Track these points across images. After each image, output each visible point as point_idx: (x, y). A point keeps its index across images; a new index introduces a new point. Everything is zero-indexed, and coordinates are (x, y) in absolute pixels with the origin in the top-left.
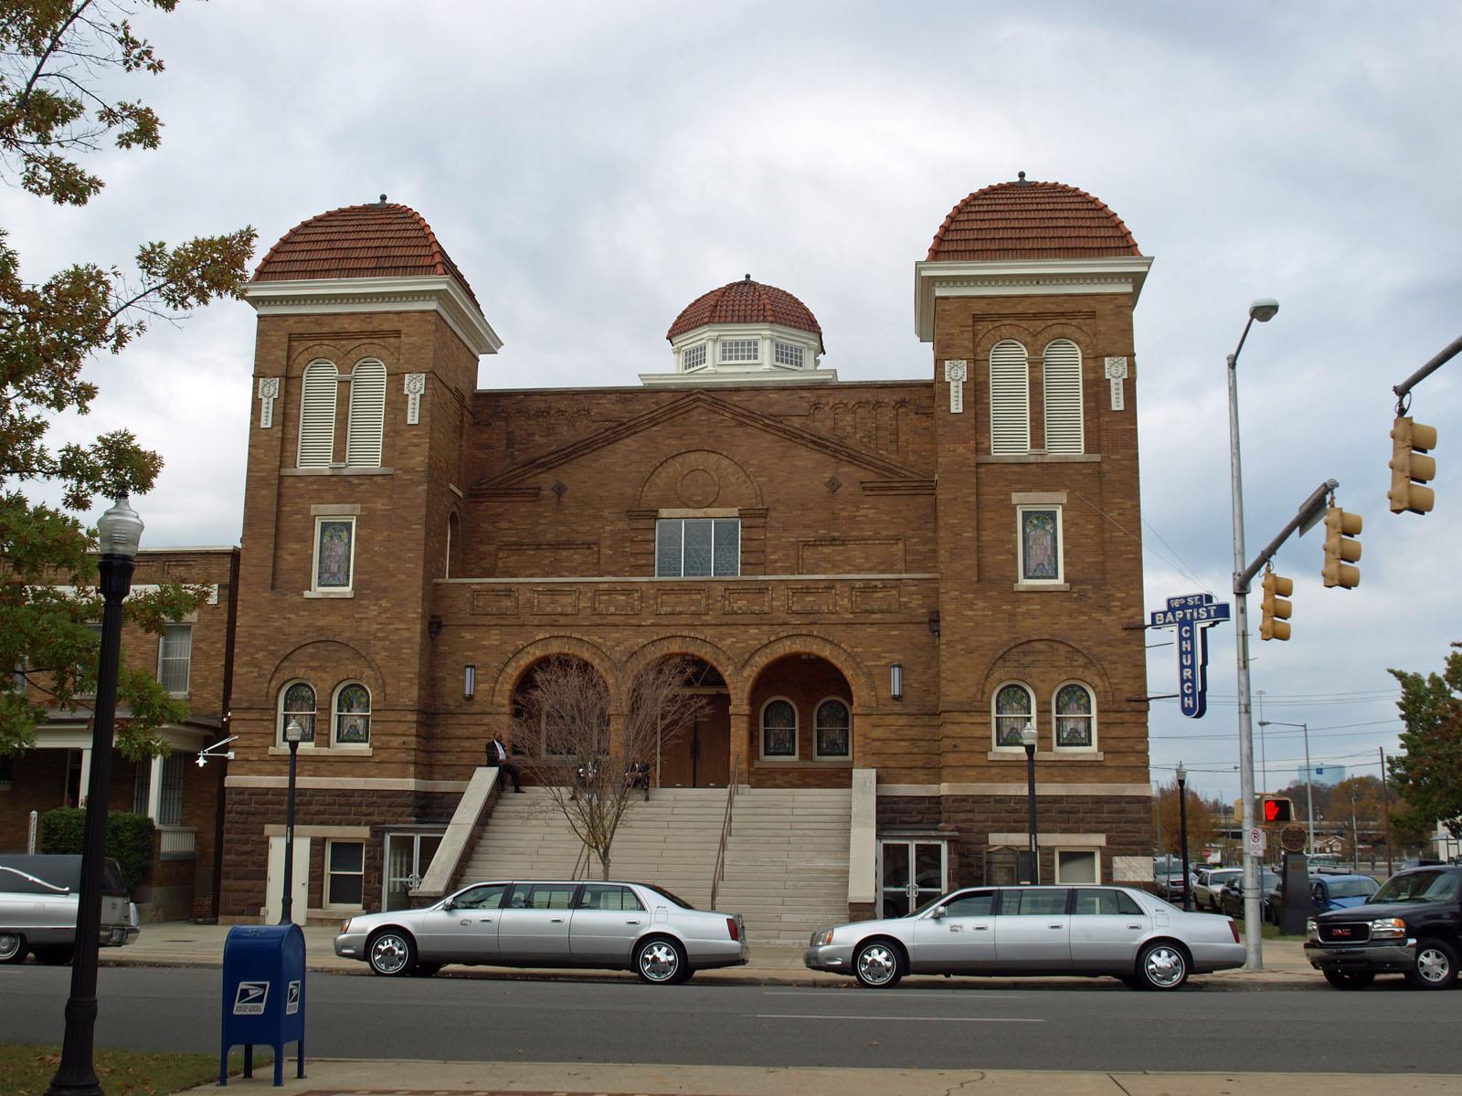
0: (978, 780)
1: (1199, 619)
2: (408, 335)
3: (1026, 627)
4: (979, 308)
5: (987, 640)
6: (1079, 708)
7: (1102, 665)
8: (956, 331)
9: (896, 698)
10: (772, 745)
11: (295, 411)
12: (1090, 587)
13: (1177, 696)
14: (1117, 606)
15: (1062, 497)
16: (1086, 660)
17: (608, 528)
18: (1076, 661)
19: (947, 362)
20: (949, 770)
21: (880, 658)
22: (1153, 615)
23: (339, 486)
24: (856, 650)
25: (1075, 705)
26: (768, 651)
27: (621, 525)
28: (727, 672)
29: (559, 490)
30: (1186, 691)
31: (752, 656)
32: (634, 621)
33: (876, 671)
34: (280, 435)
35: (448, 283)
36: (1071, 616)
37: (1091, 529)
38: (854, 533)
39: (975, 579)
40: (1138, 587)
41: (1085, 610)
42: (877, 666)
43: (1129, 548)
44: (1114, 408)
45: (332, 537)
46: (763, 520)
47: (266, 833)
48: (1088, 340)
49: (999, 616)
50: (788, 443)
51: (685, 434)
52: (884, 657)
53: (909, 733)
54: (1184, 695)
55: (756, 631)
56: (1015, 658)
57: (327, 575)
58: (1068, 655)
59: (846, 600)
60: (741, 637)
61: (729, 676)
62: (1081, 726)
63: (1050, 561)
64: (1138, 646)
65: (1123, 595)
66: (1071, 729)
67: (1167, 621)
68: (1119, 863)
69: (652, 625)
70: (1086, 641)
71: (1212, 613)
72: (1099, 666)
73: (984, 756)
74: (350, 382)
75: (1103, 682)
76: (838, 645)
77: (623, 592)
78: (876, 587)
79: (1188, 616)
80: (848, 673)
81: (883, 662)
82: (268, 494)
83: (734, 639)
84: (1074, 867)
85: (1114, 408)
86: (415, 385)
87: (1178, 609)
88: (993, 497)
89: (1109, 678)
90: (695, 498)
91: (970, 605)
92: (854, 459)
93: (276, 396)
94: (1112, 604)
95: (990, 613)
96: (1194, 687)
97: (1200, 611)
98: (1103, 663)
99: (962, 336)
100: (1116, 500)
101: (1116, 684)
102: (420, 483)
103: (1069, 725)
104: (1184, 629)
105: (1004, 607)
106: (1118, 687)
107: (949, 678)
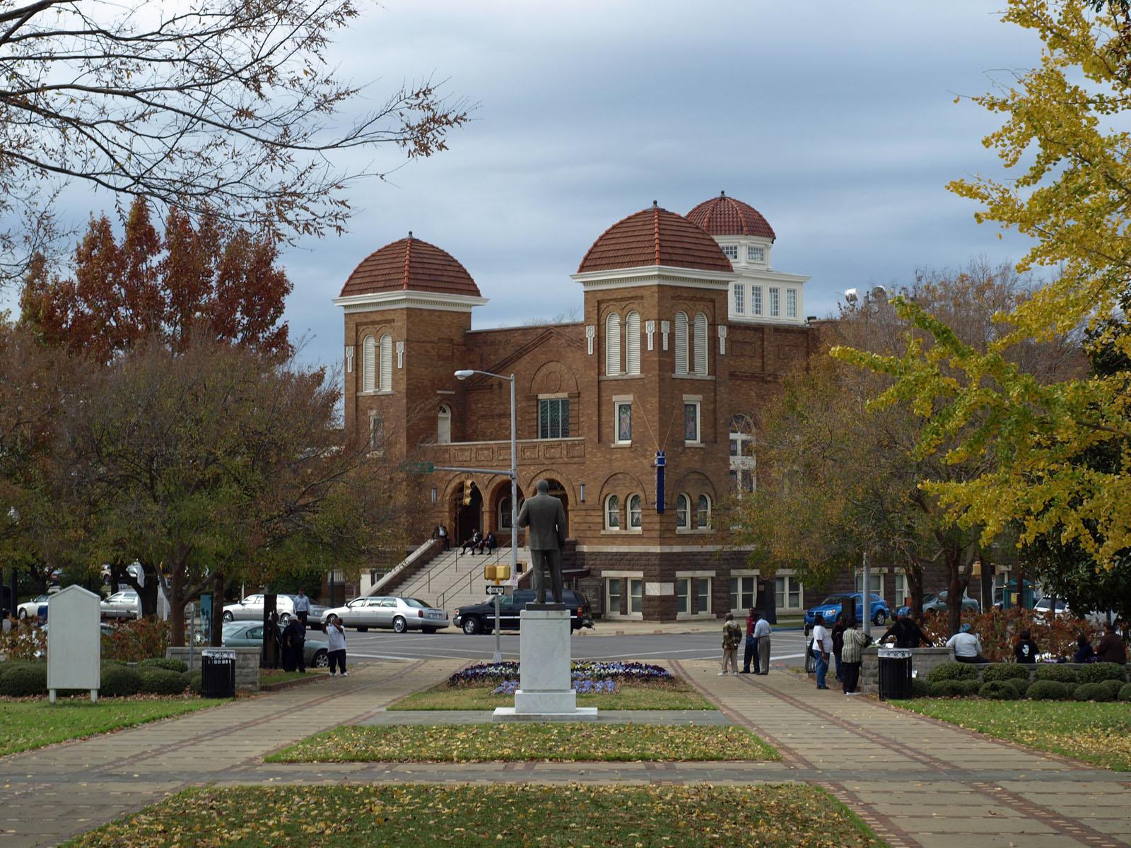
3: (617, 466)
4: (600, 296)
77: (487, 449)
86: (400, 347)
103: (636, 516)
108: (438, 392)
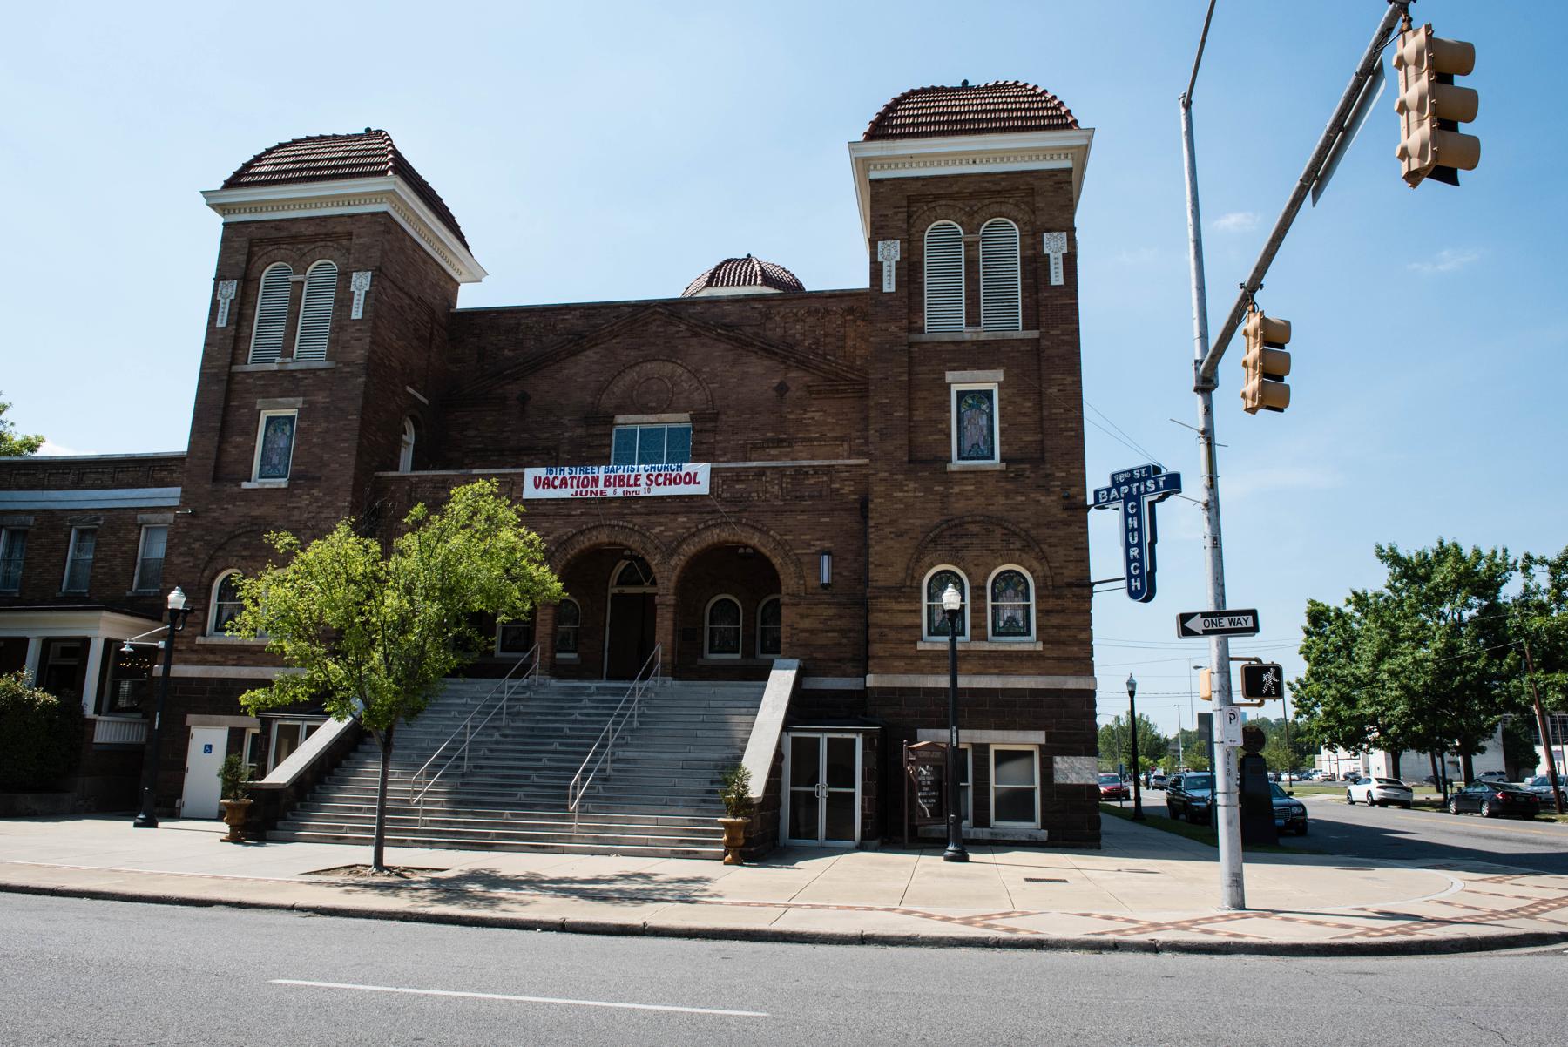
0: (906, 672)
1: (1146, 492)
2: (359, 236)
5: (918, 522)
6: (1016, 595)
7: (1041, 549)
8: (890, 212)
9: (825, 586)
10: (717, 642)
11: (250, 311)
12: (1028, 466)
13: (1124, 579)
14: (1058, 486)
15: (999, 375)
16: (1025, 543)
17: (567, 435)
18: (1013, 543)
19: (879, 243)
20: (876, 661)
21: (809, 546)
22: (1096, 493)
23: (283, 383)
24: (785, 537)
25: (1012, 592)
26: (696, 539)
27: (579, 431)
28: (654, 561)
29: (524, 399)
30: (1133, 572)
31: (679, 545)
32: (565, 511)
33: (805, 559)
34: (233, 333)
35: (395, 183)
36: (1007, 497)
37: (1029, 407)
38: (800, 435)
39: (906, 459)
40: (1079, 465)
41: (1022, 490)
42: (806, 554)
43: (1070, 425)
44: (1054, 283)
45: (275, 431)
46: (714, 424)
47: (187, 724)
48: (1026, 218)
49: (931, 497)
50: (740, 350)
51: (643, 345)
52: (814, 545)
53: (839, 623)
54: (1130, 576)
55: (685, 519)
56: (948, 541)
57: (267, 467)
58: (1005, 538)
59: (776, 487)
60: (670, 525)
61: (656, 564)
62: (1019, 615)
63: (985, 443)
64: (1080, 527)
65: (1064, 474)
66: (1008, 617)
67: (1111, 497)
68: (1060, 763)
69: (582, 514)
70: (1024, 523)
71: (1161, 484)
72: (1037, 549)
73: (912, 646)
74: (303, 283)
75: (1041, 564)
76: (767, 533)
78: (807, 473)
79: (1135, 490)
80: (776, 561)
81: (813, 550)
82: (217, 389)
83: (662, 528)
84: (1011, 768)
85: (1054, 283)
86: (361, 283)
87: (1123, 484)
88: (927, 376)
89: (1048, 562)
90: (650, 405)
91: (900, 486)
92: (802, 364)
93: (233, 297)
94: (1052, 483)
95: (922, 494)
96: (1141, 568)
97: (1148, 484)
98: (1042, 546)
99: (896, 218)
100: (1054, 376)
101: (1057, 568)
102: (358, 376)
104: (1130, 504)
105: (936, 488)
106: (1061, 571)
107: (876, 562)
108: (409, 389)
